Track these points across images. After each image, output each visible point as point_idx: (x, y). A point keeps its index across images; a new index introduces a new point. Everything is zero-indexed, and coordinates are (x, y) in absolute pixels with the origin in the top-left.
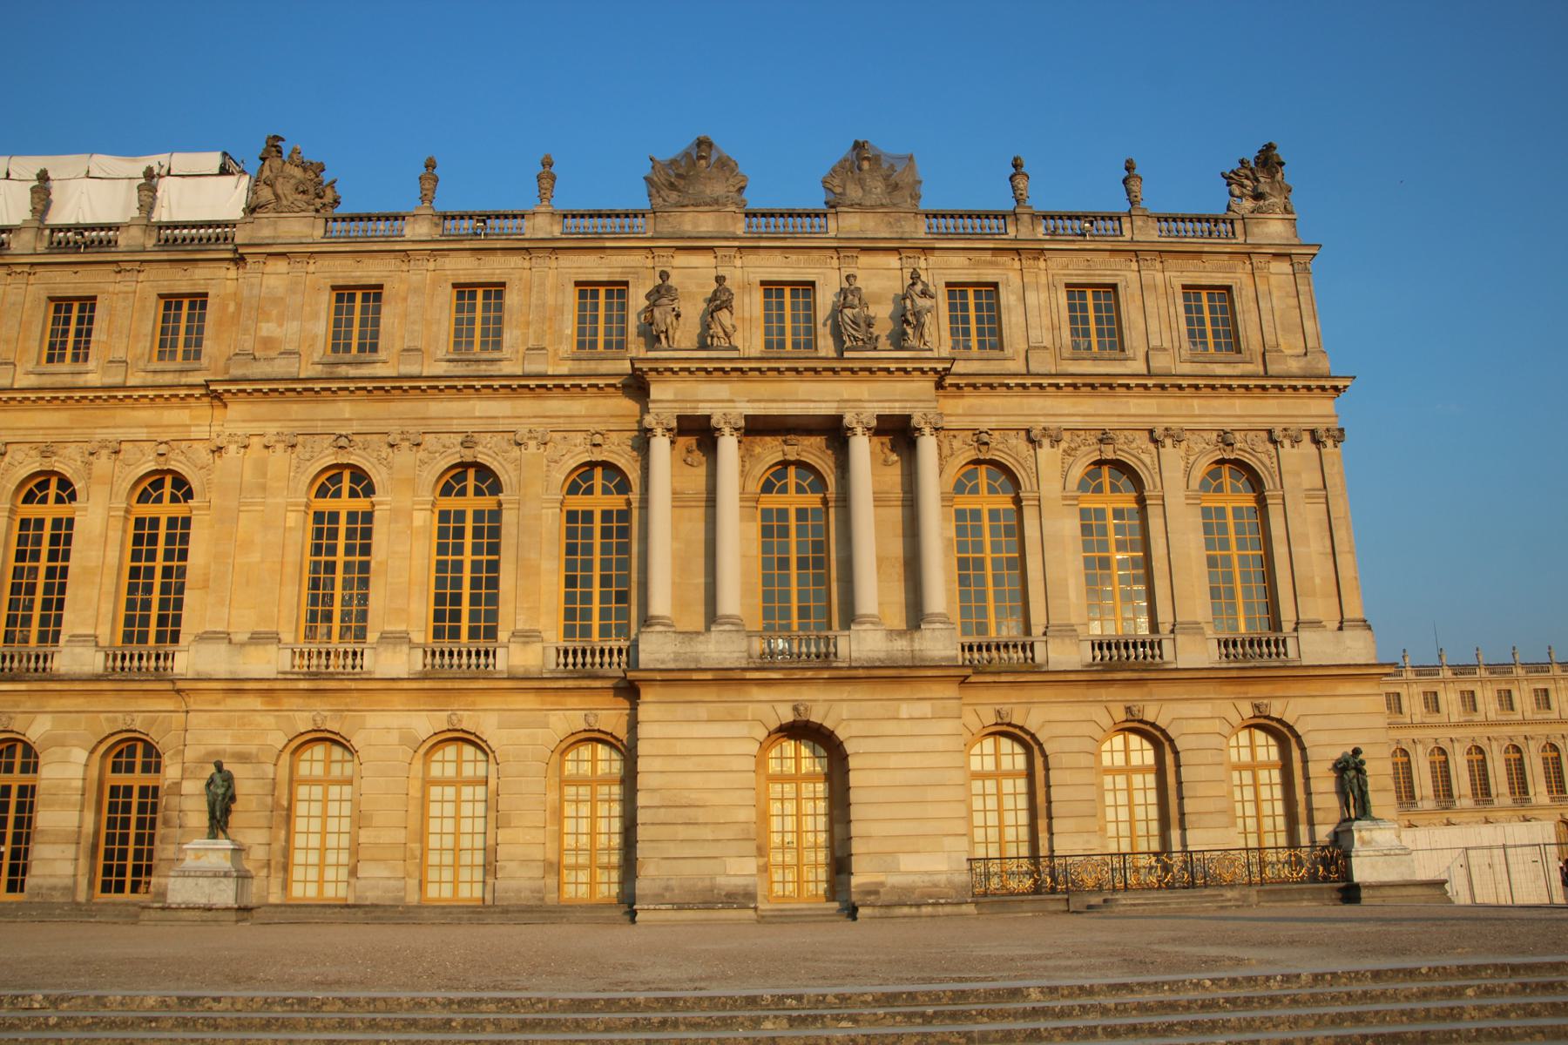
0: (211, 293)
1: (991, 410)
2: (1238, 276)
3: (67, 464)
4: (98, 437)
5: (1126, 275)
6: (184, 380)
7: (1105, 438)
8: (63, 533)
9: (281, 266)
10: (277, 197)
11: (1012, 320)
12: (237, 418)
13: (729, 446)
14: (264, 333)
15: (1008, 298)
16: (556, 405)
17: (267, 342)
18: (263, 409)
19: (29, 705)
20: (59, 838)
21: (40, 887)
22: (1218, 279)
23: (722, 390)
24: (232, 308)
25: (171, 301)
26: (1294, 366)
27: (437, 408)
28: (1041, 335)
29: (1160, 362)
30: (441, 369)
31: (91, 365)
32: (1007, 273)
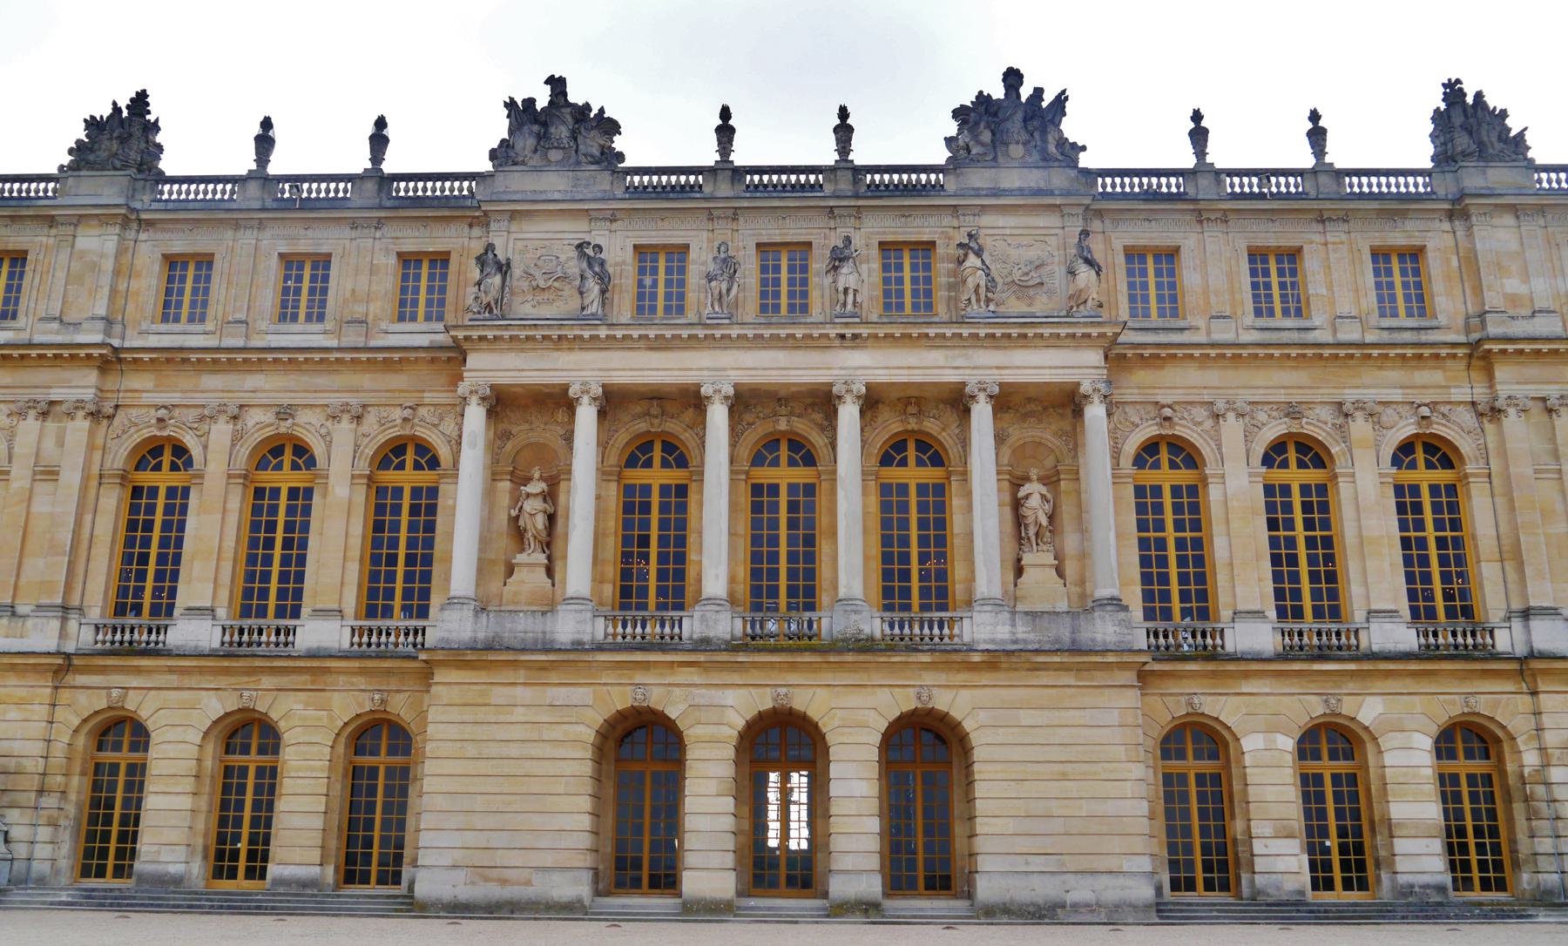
0: (1430, 245)
3: (1318, 425)
4: (1353, 398)
6: (1424, 337)
8: (1319, 505)
9: (1509, 220)
10: (1481, 146)
12: (1510, 381)
14: (1509, 290)
17: (1513, 299)
18: (1533, 370)
19: (1351, 686)
20: (1419, 830)
21: (1412, 886)
24: (1454, 262)
31: (1317, 320)
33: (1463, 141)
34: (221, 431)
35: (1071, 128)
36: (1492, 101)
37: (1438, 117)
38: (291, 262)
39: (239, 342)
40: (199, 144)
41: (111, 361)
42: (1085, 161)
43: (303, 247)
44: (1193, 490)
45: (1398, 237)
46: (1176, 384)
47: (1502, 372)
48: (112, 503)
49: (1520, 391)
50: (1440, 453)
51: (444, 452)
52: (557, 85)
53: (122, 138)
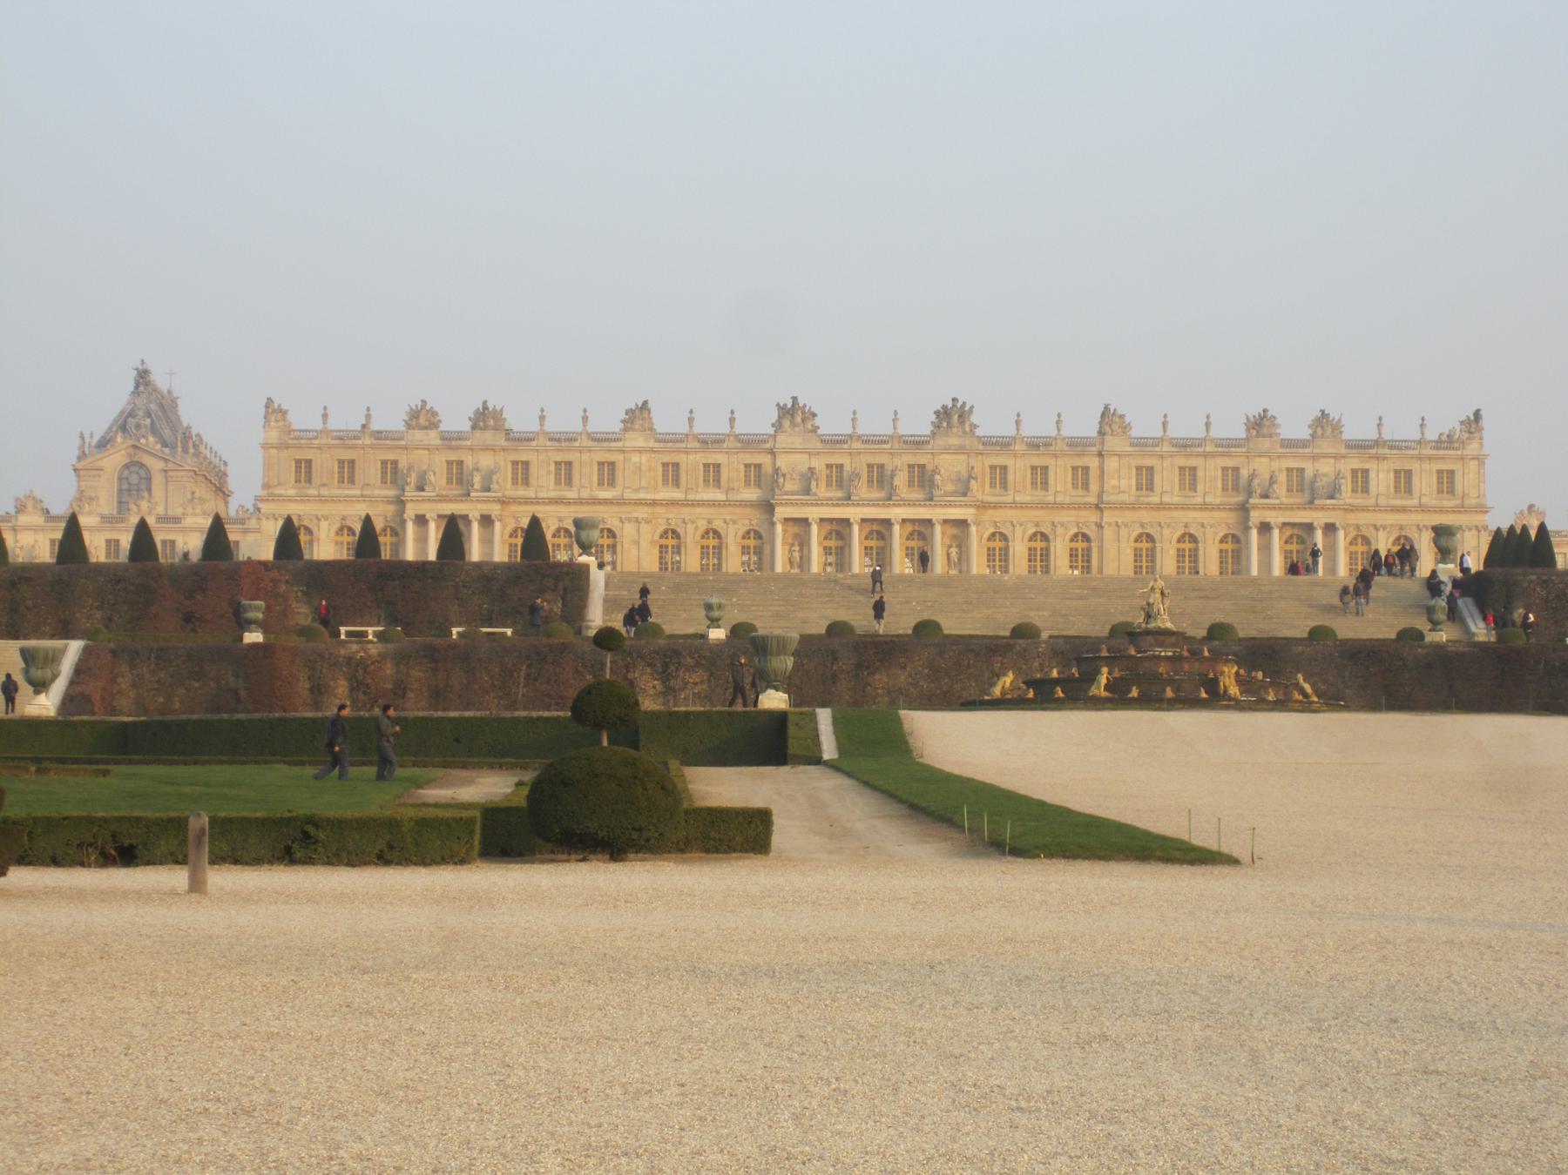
1: (1363, 519)
2: (1457, 467)
5: (1415, 466)
7: (1401, 528)
11: (1373, 484)
12: (1109, 517)
13: (1276, 533)
15: (1372, 475)
16: (1216, 514)
17: (1114, 487)
22: (1450, 467)
23: (1274, 513)
25: (1074, 468)
26: (1474, 502)
27: (1175, 514)
28: (1382, 489)
29: (1424, 500)
30: (1176, 500)
32: (1371, 466)
33: (1107, 429)
34: (690, 528)
35: (974, 419)
36: (1120, 412)
37: (1103, 415)
38: (706, 466)
39: (690, 497)
40: (667, 420)
41: (654, 503)
42: (978, 432)
43: (710, 461)
44: (1007, 548)
45: (1080, 462)
46: (1000, 515)
47: (1106, 513)
48: (656, 551)
49: (1112, 520)
50: (1086, 538)
51: (764, 535)
52: (795, 399)
53: (638, 415)
